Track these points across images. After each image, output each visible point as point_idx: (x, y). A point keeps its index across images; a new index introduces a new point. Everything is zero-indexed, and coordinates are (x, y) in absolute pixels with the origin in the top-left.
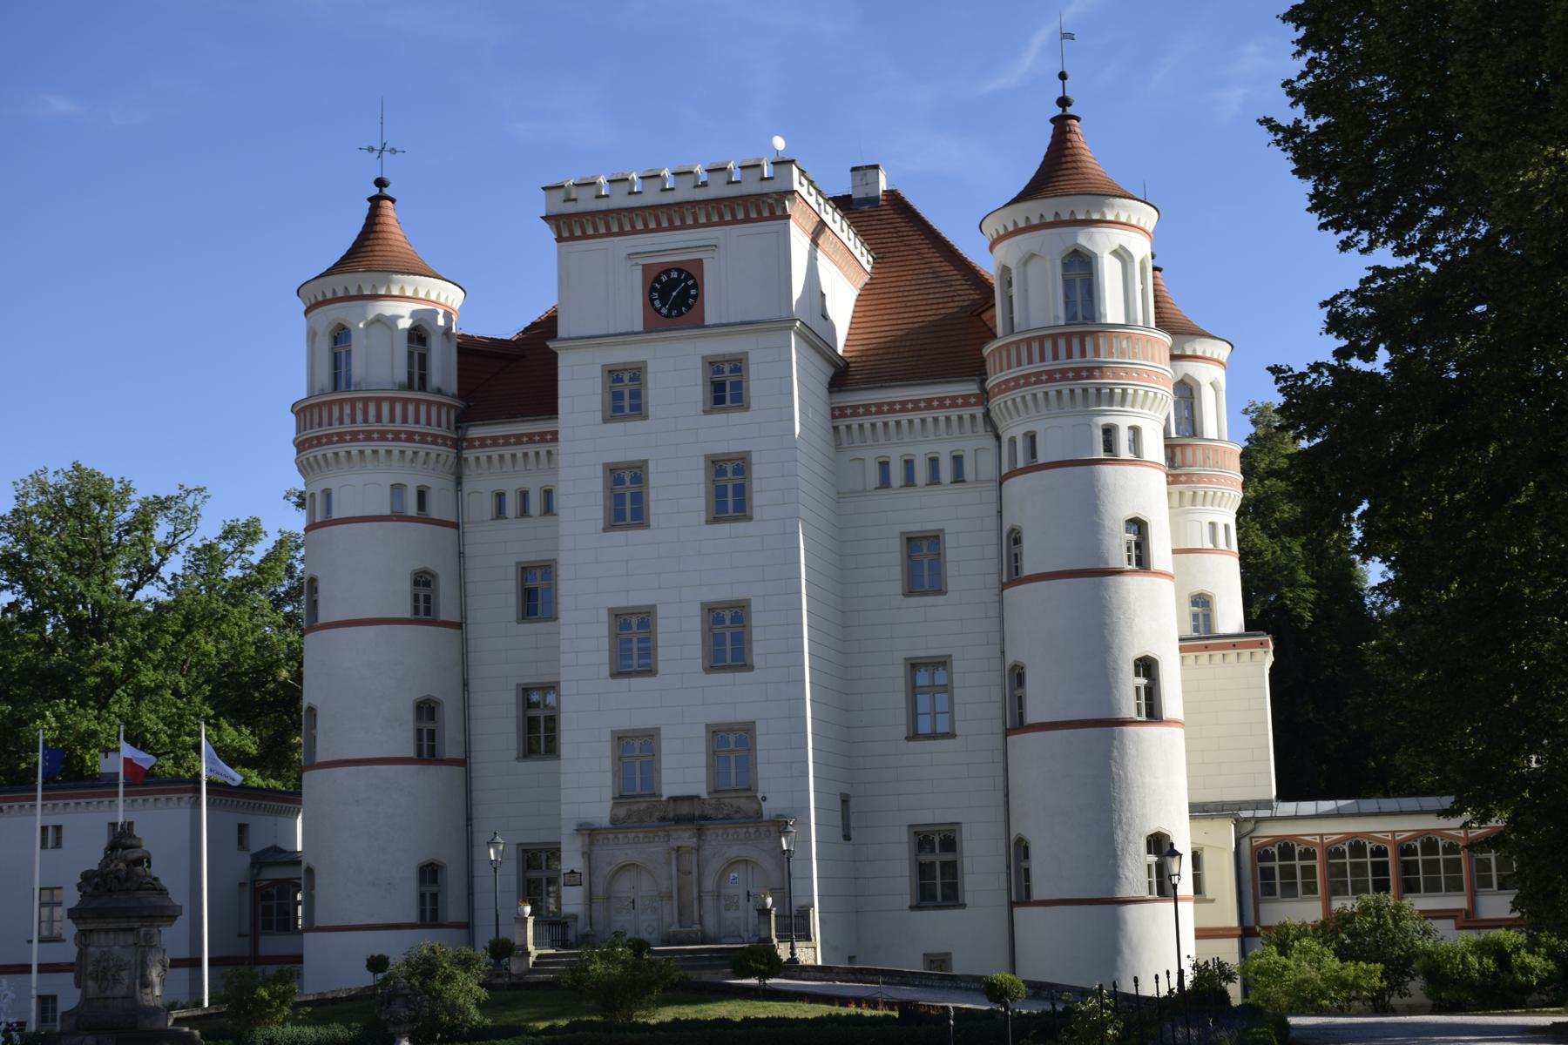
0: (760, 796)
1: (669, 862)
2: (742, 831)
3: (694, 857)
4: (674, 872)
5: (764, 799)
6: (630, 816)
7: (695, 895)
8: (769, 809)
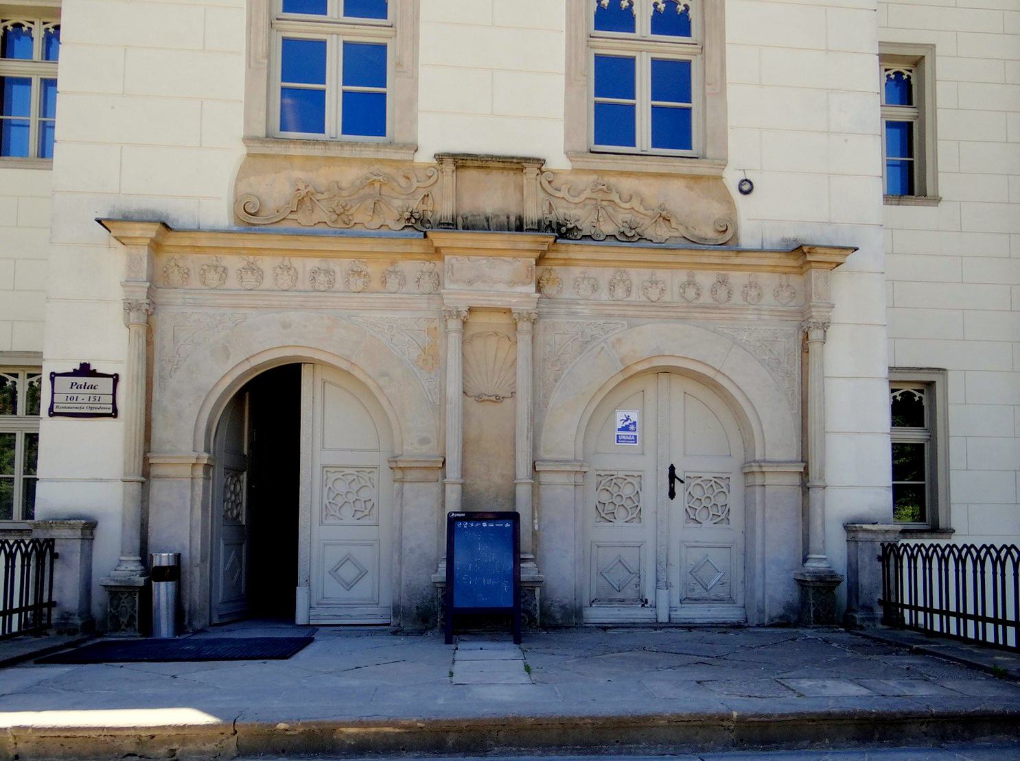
0: (732, 179)
1: (432, 359)
2: (673, 279)
3: (524, 341)
4: (453, 389)
5: (746, 188)
6: (304, 200)
7: (523, 471)
8: (760, 221)
